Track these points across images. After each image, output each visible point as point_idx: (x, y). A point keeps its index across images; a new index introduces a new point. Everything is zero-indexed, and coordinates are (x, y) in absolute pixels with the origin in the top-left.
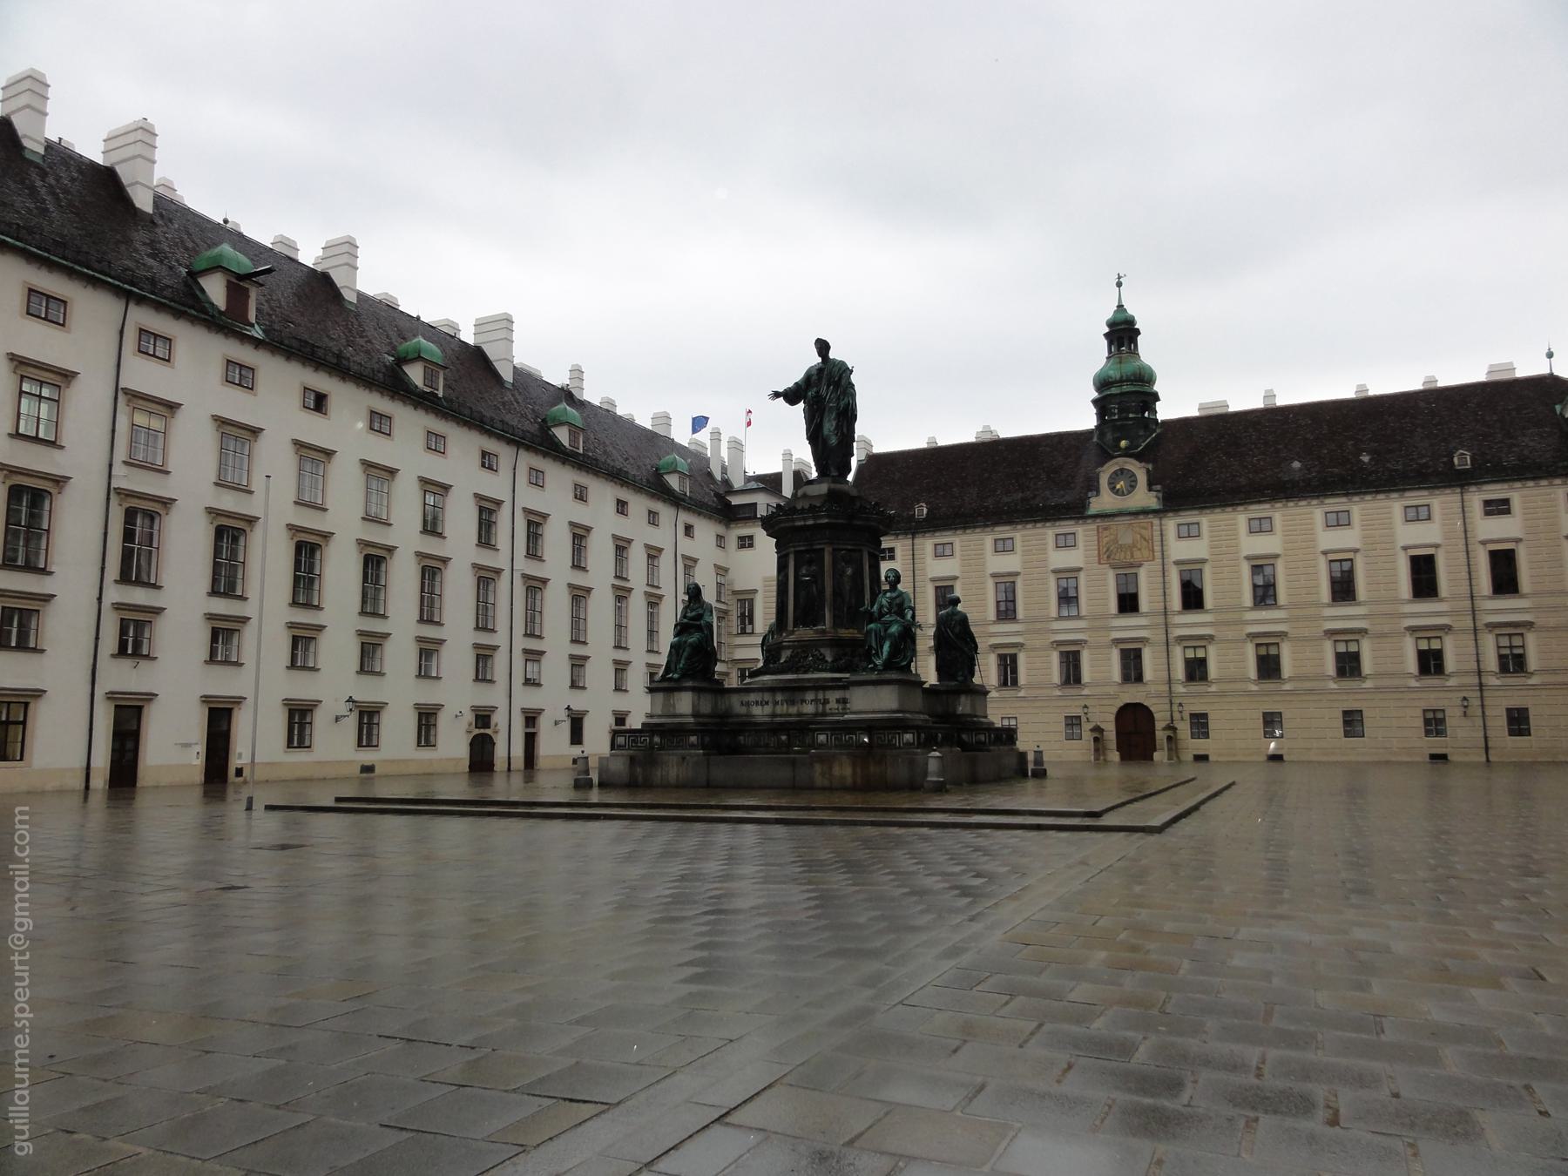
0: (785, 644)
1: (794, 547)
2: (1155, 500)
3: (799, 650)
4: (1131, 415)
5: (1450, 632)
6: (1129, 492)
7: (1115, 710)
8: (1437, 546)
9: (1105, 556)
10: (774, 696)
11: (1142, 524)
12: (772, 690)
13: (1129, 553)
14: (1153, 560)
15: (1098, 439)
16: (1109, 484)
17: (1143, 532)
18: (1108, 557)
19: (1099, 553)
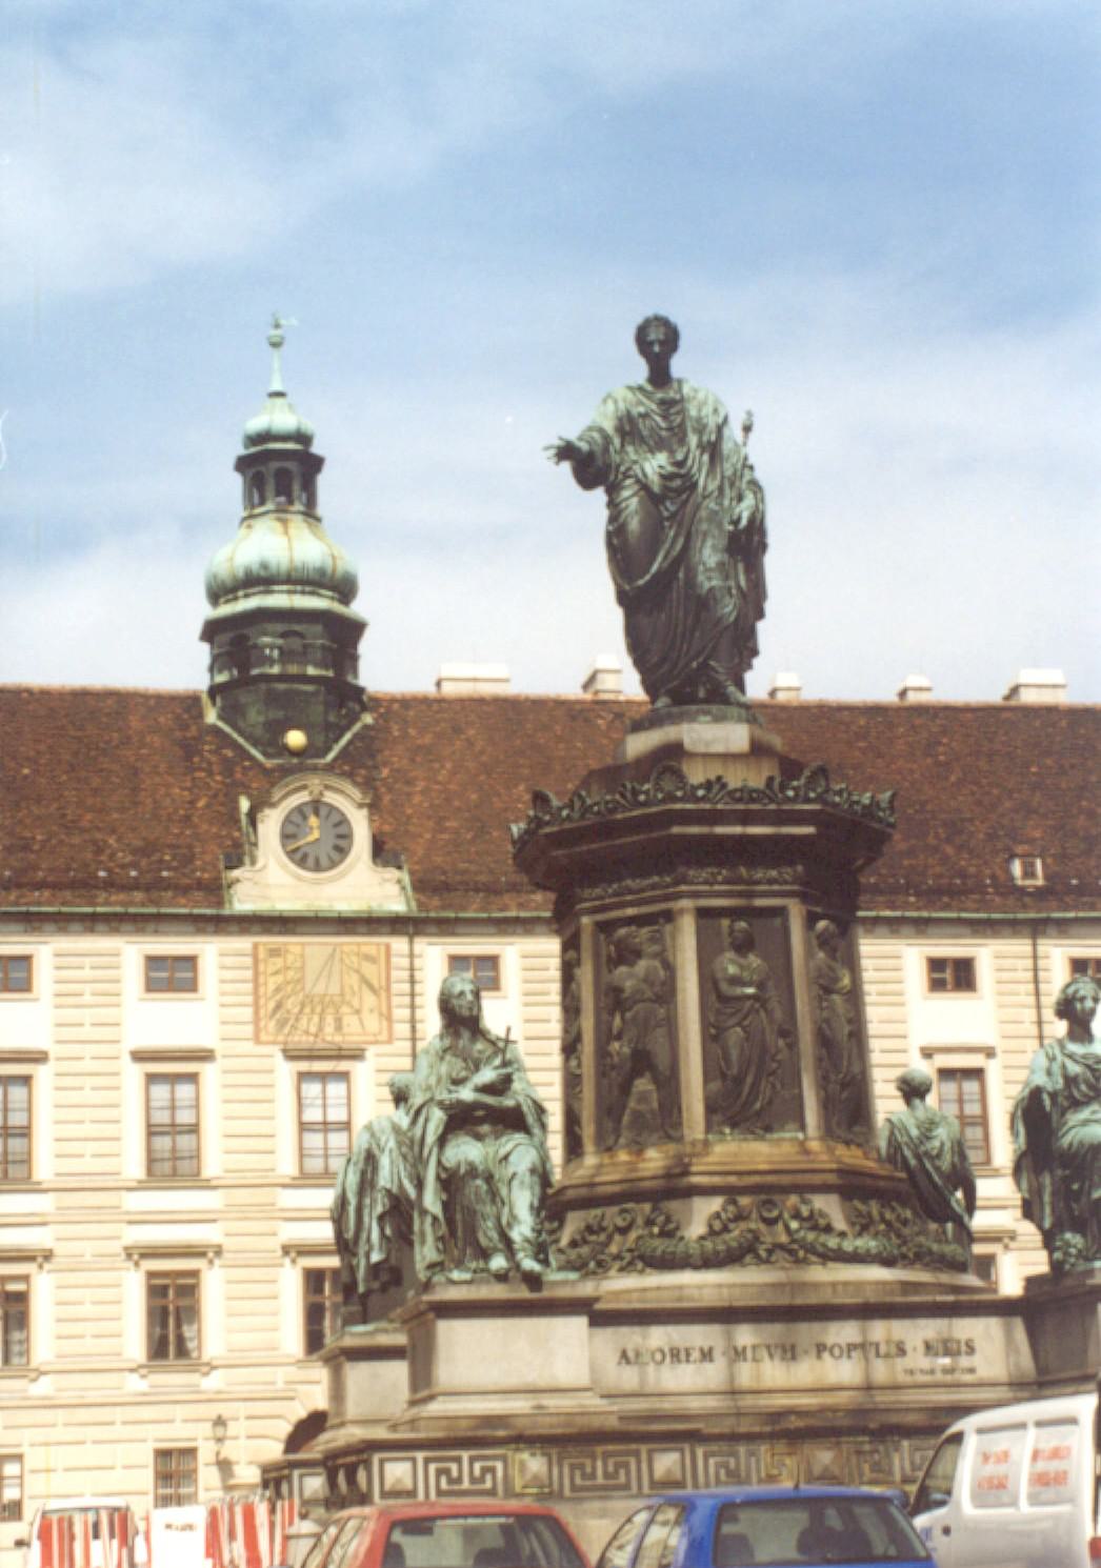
0: (695, 1180)
1: (695, 895)
2: (395, 889)
3: (744, 1201)
4: (311, 671)
5: (1012, 1245)
6: (333, 865)
7: (285, 1429)
8: (990, 1053)
9: (272, 1025)
10: (729, 1337)
11: (364, 949)
12: (725, 1315)
13: (330, 1019)
14: (390, 1041)
15: (220, 717)
16: (286, 837)
17: (369, 970)
18: (282, 1024)
19: (256, 1013)
